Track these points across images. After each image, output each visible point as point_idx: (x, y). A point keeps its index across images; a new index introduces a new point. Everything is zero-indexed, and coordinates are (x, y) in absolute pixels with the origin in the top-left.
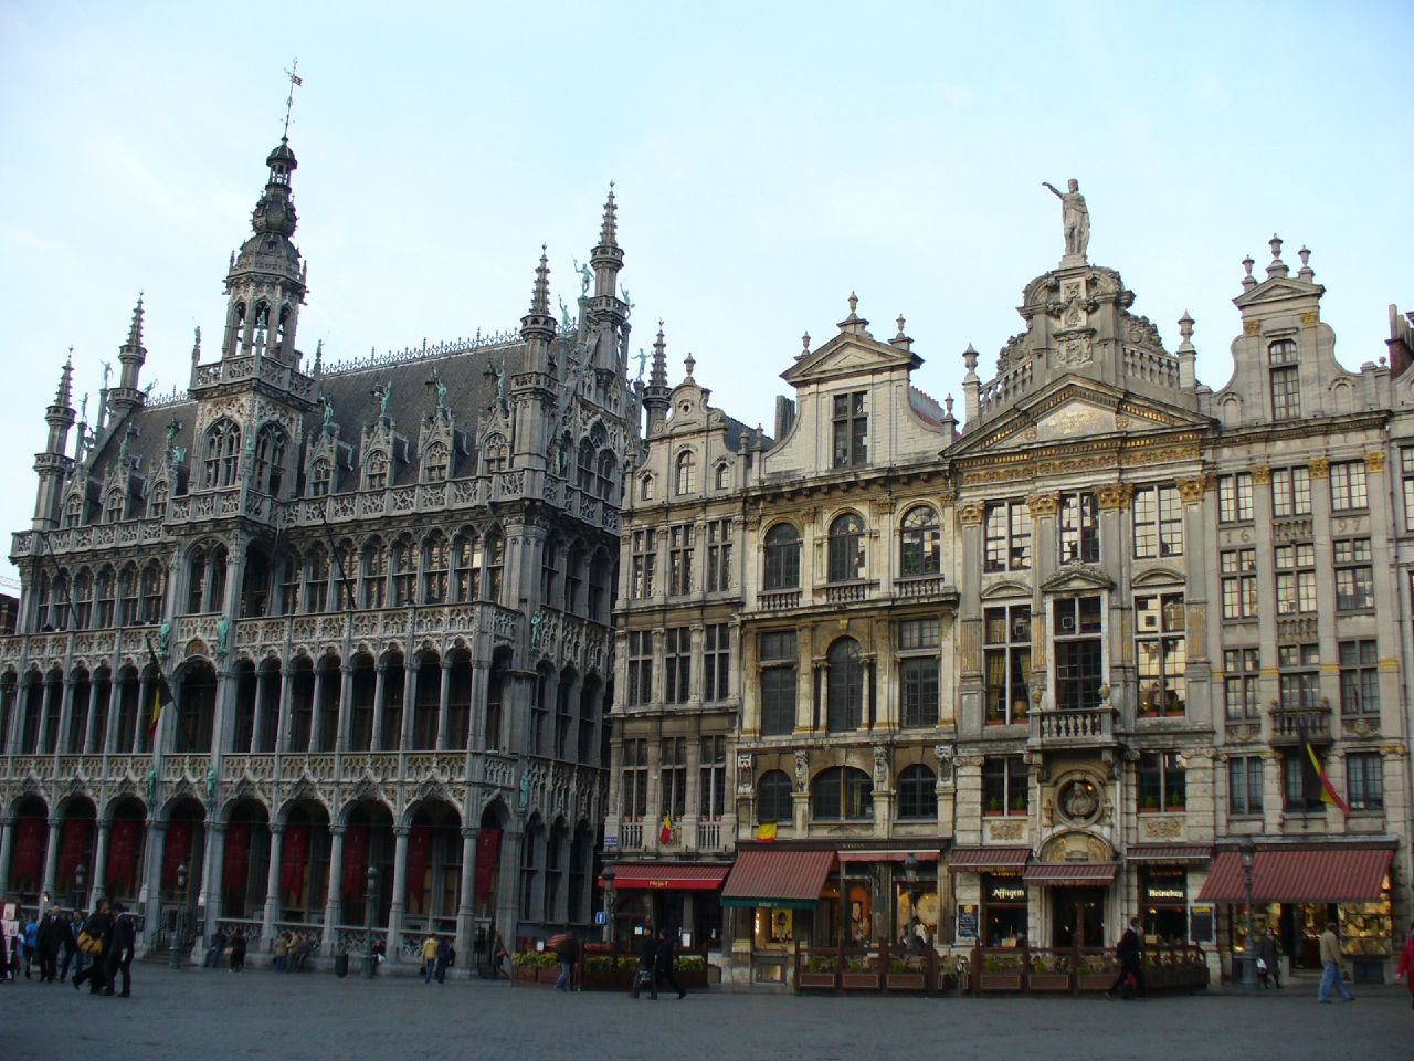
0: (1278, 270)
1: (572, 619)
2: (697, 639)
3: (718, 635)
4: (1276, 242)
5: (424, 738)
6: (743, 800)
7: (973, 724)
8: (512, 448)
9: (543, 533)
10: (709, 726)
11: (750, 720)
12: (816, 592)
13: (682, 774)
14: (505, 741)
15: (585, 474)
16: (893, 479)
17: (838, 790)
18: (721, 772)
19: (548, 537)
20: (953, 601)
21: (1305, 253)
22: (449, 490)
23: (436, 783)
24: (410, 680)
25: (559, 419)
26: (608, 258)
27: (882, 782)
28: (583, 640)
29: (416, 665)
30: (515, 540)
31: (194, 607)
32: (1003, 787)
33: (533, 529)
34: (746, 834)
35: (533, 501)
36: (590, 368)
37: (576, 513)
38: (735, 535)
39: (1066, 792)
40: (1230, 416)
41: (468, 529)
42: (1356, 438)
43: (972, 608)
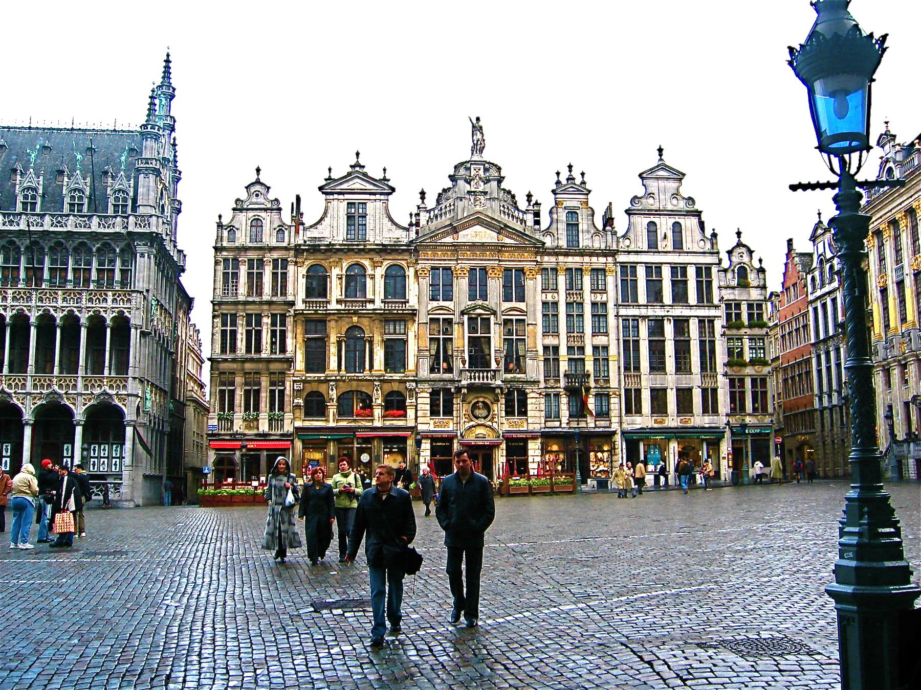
0: (570, 179)
2: (266, 321)
3: (279, 320)
4: (570, 167)
6: (298, 406)
7: (424, 373)
10: (274, 367)
11: (300, 364)
12: (339, 302)
13: (257, 392)
16: (384, 250)
17: (355, 401)
18: (282, 393)
20: (413, 313)
21: (583, 174)
23: (107, 394)
27: (378, 399)
32: (442, 403)
34: (298, 424)
35: (157, 234)
38: (291, 268)
39: (475, 407)
40: (548, 242)
41: (106, 245)
42: (602, 260)
43: (423, 318)
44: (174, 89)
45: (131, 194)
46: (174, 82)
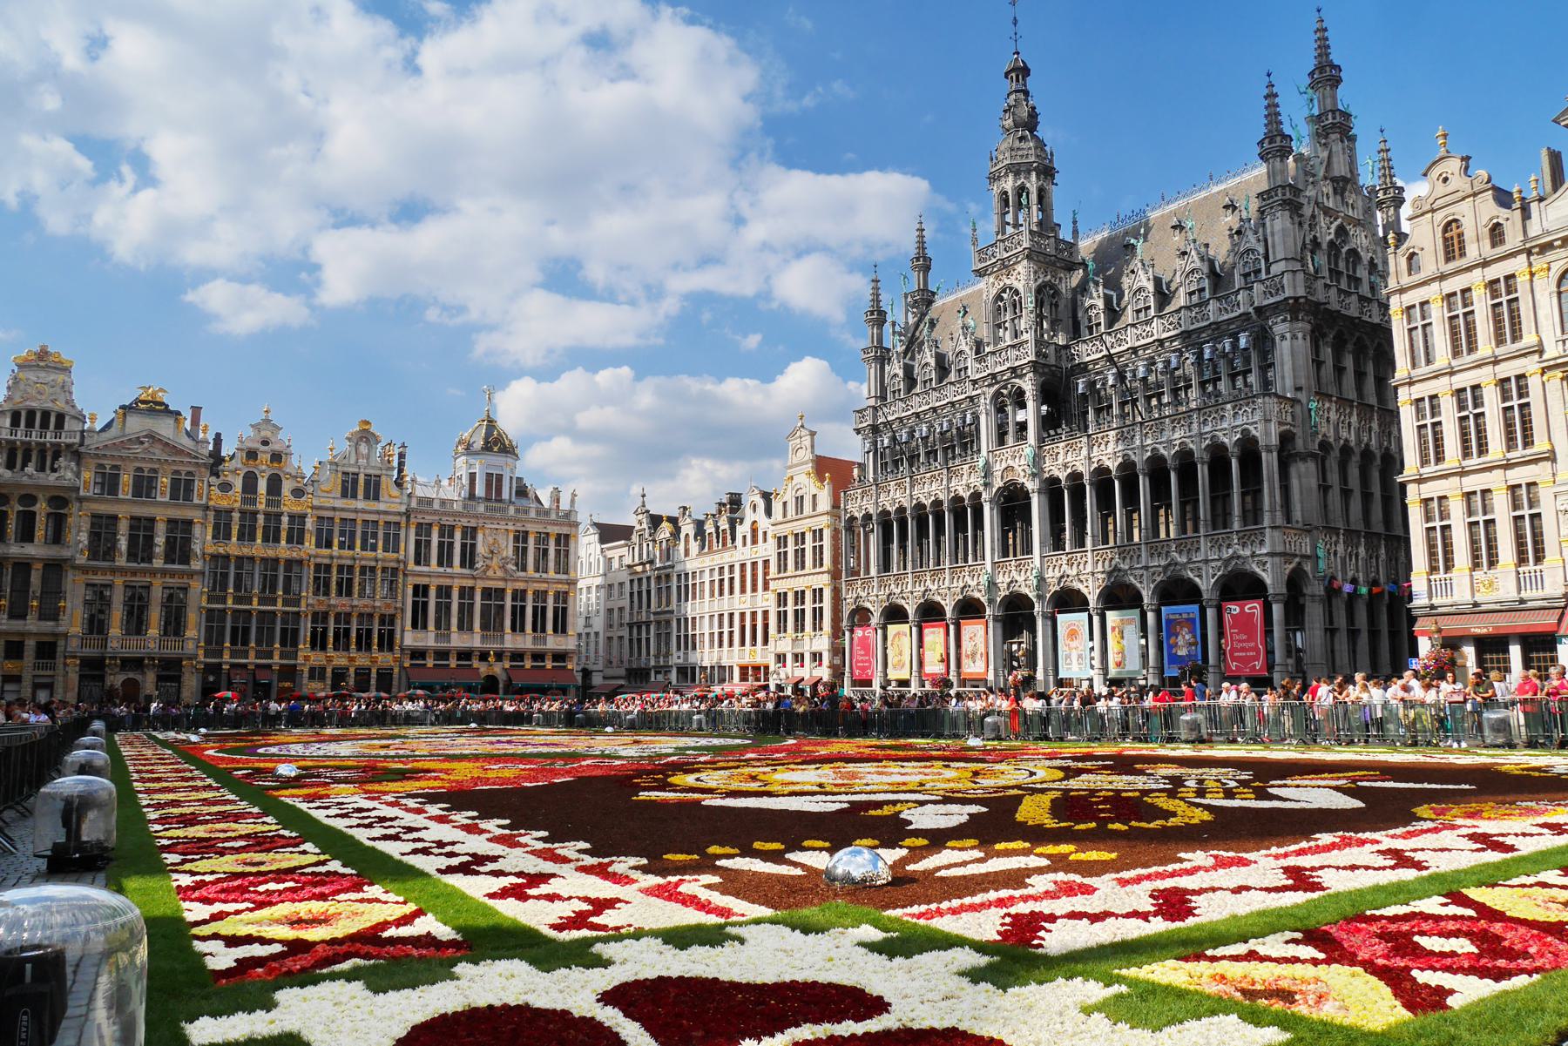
1: (1343, 401)
5: (1220, 518)
8: (1267, 258)
9: (1308, 327)
14: (1297, 514)
15: (1335, 273)
19: (1313, 331)
22: (1213, 306)
23: (1239, 557)
24: (1203, 472)
25: (1306, 226)
26: (1326, 75)
28: (1354, 419)
29: (1206, 457)
30: (1283, 338)
31: (1001, 441)
33: (1300, 325)
35: (1296, 299)
36: (1325, 178)
37: (1334, 306)
44: (1338, 68)
45: (1262, 251)
46: (1335, 58)
